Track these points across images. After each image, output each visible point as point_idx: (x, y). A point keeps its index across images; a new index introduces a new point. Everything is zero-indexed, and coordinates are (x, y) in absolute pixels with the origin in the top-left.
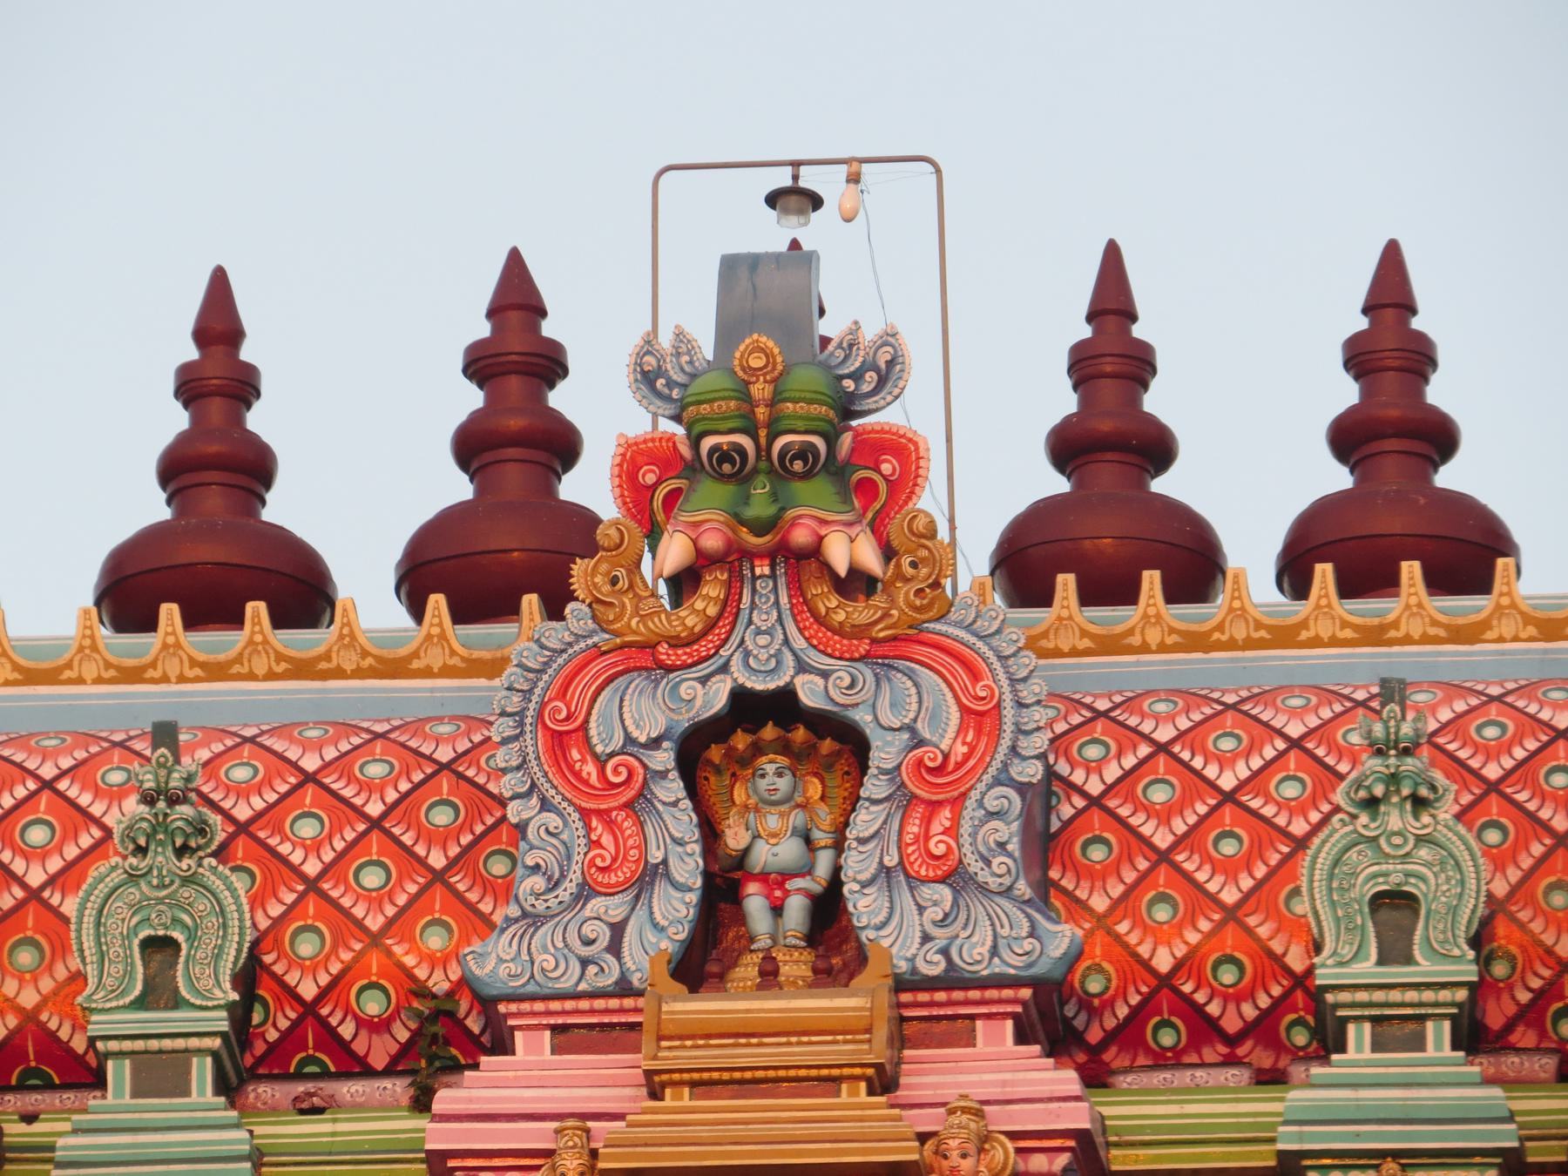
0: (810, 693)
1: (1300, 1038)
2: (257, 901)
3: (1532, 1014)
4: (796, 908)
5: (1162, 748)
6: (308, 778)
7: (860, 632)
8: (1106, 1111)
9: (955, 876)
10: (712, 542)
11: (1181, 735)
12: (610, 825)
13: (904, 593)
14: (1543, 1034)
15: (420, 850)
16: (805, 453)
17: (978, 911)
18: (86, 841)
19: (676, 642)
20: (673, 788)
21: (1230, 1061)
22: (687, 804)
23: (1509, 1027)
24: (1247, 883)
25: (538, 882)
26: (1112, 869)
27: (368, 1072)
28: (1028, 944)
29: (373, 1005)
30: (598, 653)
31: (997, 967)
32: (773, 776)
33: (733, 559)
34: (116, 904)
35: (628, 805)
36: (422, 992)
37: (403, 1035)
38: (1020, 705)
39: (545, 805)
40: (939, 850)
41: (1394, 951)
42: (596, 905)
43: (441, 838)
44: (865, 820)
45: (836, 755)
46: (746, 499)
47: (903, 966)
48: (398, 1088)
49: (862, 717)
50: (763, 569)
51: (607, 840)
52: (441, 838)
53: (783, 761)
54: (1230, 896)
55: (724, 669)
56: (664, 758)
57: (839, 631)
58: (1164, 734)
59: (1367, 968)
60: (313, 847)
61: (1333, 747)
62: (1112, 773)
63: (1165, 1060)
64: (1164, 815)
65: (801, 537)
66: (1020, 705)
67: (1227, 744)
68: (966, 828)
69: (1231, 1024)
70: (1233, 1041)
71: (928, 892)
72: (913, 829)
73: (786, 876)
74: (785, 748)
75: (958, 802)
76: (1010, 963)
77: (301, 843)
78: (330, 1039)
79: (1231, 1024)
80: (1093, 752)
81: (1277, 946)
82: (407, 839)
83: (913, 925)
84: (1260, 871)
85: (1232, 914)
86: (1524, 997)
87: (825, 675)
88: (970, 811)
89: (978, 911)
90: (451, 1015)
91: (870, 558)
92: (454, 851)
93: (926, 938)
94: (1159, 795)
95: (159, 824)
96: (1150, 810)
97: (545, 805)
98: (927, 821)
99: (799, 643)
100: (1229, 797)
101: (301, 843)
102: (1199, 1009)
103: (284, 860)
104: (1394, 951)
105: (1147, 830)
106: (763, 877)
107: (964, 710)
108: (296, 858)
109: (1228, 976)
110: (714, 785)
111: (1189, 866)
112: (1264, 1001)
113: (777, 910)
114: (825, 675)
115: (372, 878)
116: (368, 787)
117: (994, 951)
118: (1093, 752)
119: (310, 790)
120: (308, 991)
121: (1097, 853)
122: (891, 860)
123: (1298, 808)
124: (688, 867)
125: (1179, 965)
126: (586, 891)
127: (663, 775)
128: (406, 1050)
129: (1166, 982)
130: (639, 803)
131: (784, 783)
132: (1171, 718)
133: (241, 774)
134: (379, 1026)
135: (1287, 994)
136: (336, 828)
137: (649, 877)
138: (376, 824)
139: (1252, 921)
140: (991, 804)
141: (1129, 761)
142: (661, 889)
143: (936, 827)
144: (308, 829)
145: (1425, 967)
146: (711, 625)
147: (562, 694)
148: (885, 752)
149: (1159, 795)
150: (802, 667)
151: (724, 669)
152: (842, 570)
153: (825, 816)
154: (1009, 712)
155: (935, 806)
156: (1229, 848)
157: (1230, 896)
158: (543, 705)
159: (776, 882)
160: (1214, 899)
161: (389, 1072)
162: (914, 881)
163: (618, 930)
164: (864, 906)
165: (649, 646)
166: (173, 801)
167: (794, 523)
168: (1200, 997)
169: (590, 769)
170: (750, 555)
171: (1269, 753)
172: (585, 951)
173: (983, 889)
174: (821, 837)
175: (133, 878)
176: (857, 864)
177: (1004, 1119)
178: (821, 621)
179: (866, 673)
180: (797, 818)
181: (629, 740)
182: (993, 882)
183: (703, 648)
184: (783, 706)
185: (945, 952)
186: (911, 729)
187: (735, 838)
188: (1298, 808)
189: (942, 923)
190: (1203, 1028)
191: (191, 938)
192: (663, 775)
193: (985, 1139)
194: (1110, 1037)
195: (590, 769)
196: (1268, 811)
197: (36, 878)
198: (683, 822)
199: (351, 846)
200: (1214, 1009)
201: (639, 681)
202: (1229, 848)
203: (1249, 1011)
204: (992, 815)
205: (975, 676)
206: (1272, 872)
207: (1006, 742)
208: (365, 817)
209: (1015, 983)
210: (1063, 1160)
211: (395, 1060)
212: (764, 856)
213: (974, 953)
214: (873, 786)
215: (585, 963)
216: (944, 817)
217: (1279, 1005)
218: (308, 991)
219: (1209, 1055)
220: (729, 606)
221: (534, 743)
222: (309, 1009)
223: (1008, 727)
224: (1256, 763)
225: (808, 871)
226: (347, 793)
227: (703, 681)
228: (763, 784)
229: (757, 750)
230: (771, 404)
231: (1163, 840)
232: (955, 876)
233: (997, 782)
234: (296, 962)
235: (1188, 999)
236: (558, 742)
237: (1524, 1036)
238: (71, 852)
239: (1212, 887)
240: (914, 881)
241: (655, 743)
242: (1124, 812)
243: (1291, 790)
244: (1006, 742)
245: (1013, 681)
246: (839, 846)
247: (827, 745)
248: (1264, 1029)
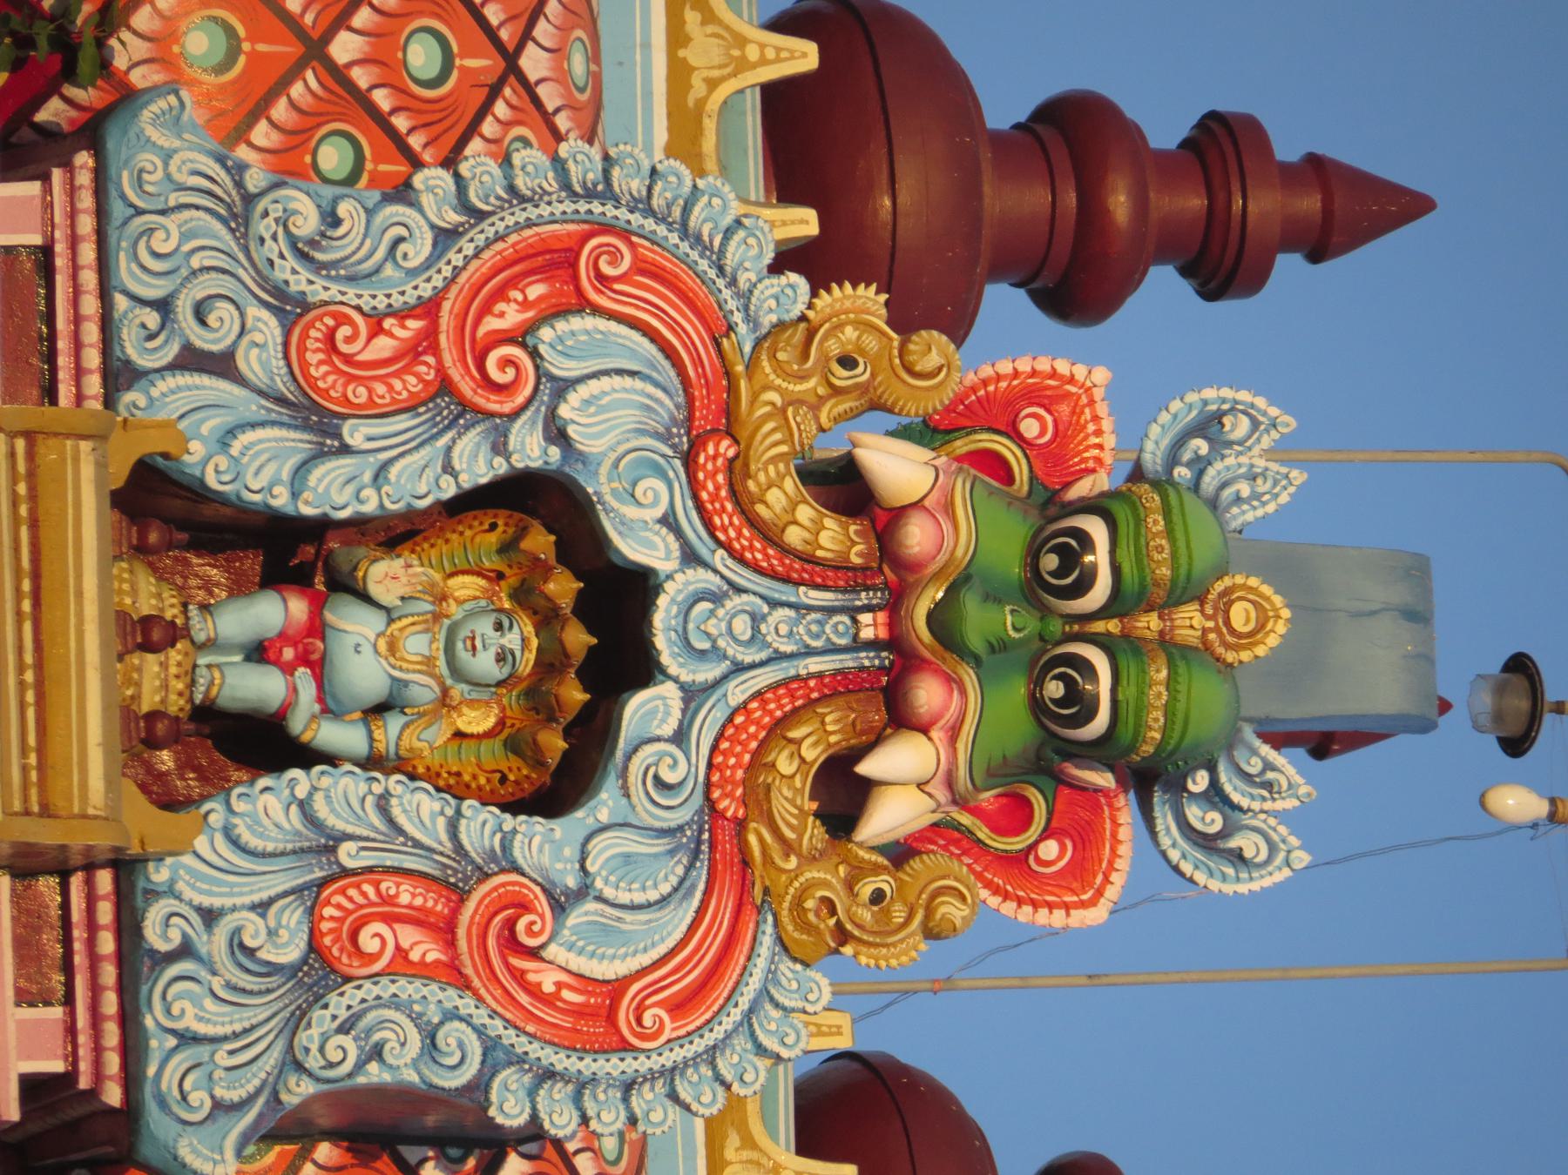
7: (757, 799)
10: (917, 536)
12: (412, 352)
13: (827, 878)
19: (737, 470)
22: (449, 490)
25: (307, 222)
28: (199, 1098)
30: (719, 330)
31: (158, 1044)
35: (445, 385)
38: (628, 1087)
39: (445, 237)
40: (368, 943)
42: (267, 327)
46: (993, 597)
47: (159, 875)
49: (605, 804)
50: (871, 627)
51: (383, 347)
53: (527, 662)
55: (691, 557)
57: (759, 762)
65: (927, 694)
66: (628, 1087)
68: (408, 988)
71: (292, 918)
72: (406, 894)
73: (319, 667)
74: (550, 664)
75: (452, 973)
88: (436, 997)
90: (69, 73)
92: (361, 77)
93: (210, 917)
97: (445, 237)
98: (418, 919)
99: (737, 692)
106: (317, 628)
113: (259, 652)
114: (680, 737)
117: (187, 1039)
122: (349, 856)
127: (500, 448)
131: (484, 664)
140: (451, 1034)
142: (297, 442)
143: (408, 935)
146: (769, 534)
147: (644, 268)
150: (693, 695)
151: (691, 557)
152: (866, 768)
153: (427, 740)
154: (614, 1066)
155: (445, 931)
158: (625, 234)
162: (313, 894)
163: (222, 365)
165: (729, 423)
167: (952, 681)
169: (509, 316)
170: (895, 604)
172: (184, 308)
173: (298, 1020)
178: (778, 729)
180: (423, 690)
181: (563, 387)
182: (309, 1037)
183: (728, 519)
185: (185, 950)
186: (583, 892)
189: (241, 949)
192: (500, 448)
195: (509, 316)
201: (668, 405)
209: (131, 1078)
215: (164, 306)
216: (427, 950)
223: (587, 1065)
225: (329, 708)
227: (669, 521)
228: (484, 626)
229: (547, 618)
230: (1167, 643)
233: (490, 1045)
240: (313, 894)
241: (557, 434)
245: (670, 1073)
246: (373, 762)
247: (554, 743)
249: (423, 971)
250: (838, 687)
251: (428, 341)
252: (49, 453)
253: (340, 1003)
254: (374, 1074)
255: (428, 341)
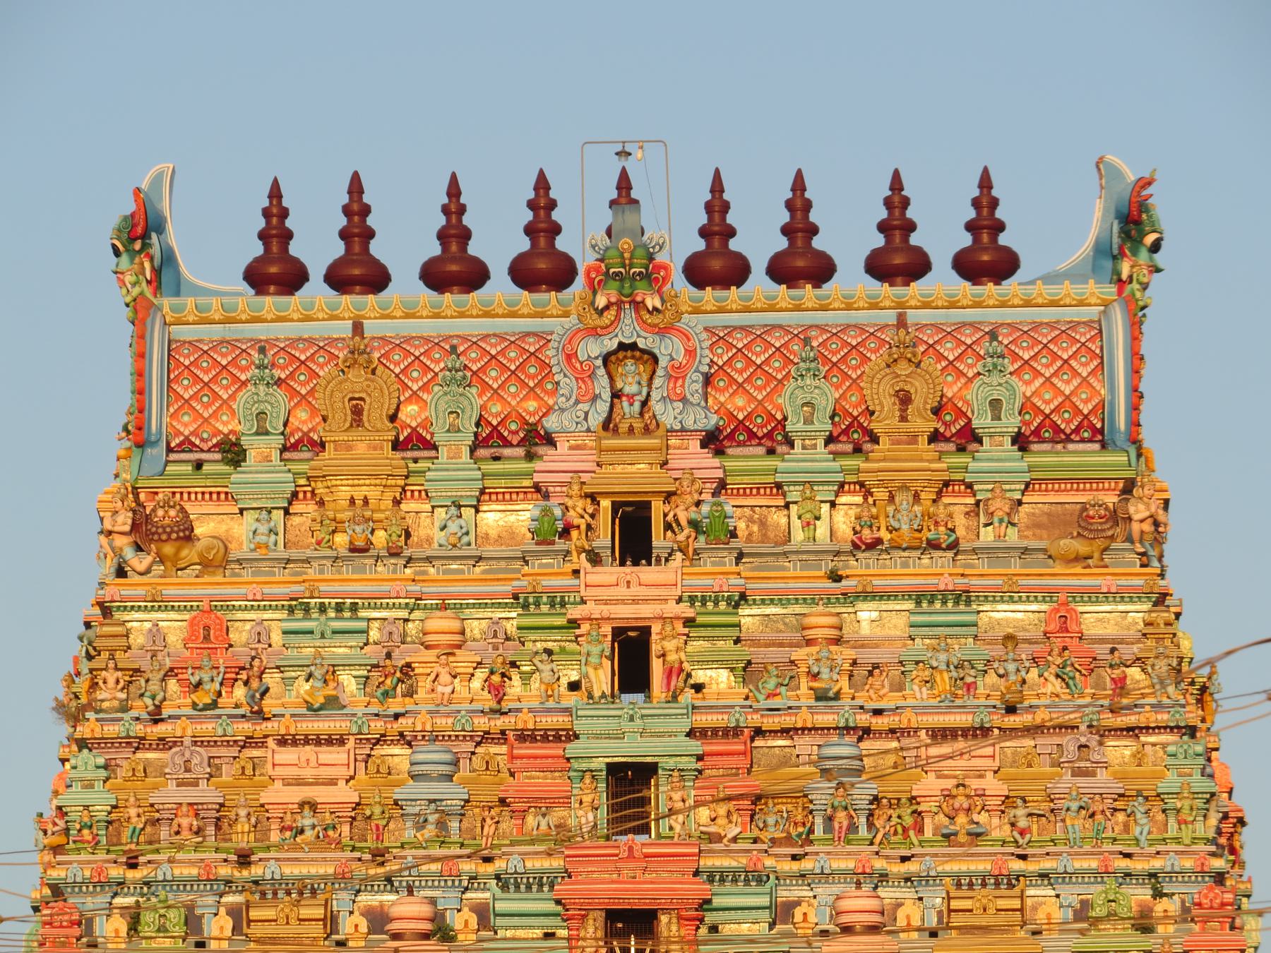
0: (641, 344)
1: (779, 438)
2: (480, 396)
3: (845, 432)
4: (637, 405)
5: (739, 350)
6: (493, 357)
7: (655, 326)
8: (726, 464)
9: (683, 399)
10: (613, 300)
11: (745, 346)
12: (584, 382)
13: (668, 314)
14: (849, 438)
15: (526, 381)
16: (641, 273)
17: (690, 410)
18: (429, 377)
19: (602, 328)
20: (601, 371)
21: (759, 444)
22: (606, 376)
23: (839, 435)
24: (764, 393)
25: (563, 399)
26: (726, 389)
27: (512, 445)
28: (705, 420)
29: (513, 427)
30: (579, 330)
31: (696, 427)
32: (630, 366)
33: (619, 304)
34: (441, 401)
35: (589, 376)
36: (527, 423)
37: (522, 435)
38: (702, 348)
39: (565, 376)
40: (679, 392)
41: (808, 421)
42: (580, 406)
43: (532, 377)
44: (657, 382)
45: (648, 360)
47: (669, 427)
48: (520, 451)
49: (656, 351)
50: (627, 306)
51: (583, 386)
52: (532, 377)
53: (633, 361)
54: (760, 397)
55: (616, 336)
56: (599, 362)
57: (649, 325)
58: (740, 345)
59: (800, 426)
60: (496, 379)
61: (789, 350)
62: (725, 358)
63: (740, 444)
64: (741, 372)
65: (639, 299)
66: (702, 348)
67: (758, 349)
68: (686, 385)
69: (760, 434)
70: (760, 439)
71: (676, 404)
72: (671, 385)
73: (634, 395)
74: (633, 357)
75: (684, 378)
76: (700, 426)
77: (492, 378)
78: (501, 436)
79: (760, 434)
80: (720, 351)
81: (773, 412)
82: (523, 377)
83: (672, 414)
84: (768, 390)
85: (760, 402)
86: (844, 427)
87: (646, 338)
88: (688, 380)
89: (690, 410)
90: (536, 430)
91: (658, 304)
92: (536, 381)
93: (675, 418)
94: (739, 365)
95: (453, 378)
96: (736, 370)
97: (565, 376)
98: (675, 383)
99: (638, 328)
100: (759, 366)
101: (492, 378)
102: (751, 430)
103: (487, 384)
104: (808, 421)
105: (736, 377)
106: (627, 396)
107: (686, 350)
108: (490, 383)
109: (759, 420)
110: (612, 367)
111: (748, 388)
112: (769, 428)
113: (631, 404)
114: (646, 338)
115: (513, 389)
116: (510, 360)
117: (695, 422)
118: (720, 351)
119: (494, 361)
120: (495, 423)
121: (722, 384)
122: (665, 395)
123: (779, 370)
124: (607, 395)
125: (745, 418)
126: (577, 402)
128: (522, 440)
129: (741, 422)
130: (592, 376)
131: (633, 368)
132: (742, 340)
133: (473, 355)
134: (516, 433)
135: (776, 426)
136: (502, 374)
137: (595, 398)
138: (513, 372)
139: (766, 405)
140: (694, 379)
141: (730, 354)
142: (599, 401)
143: (678, 385)
144: (493, 373)
145: (817, 426)
148: (663, 362)
149: (739, 365)
150: (639, 336)
151: (616, 336)
153: (645, 377)
154: (698, 351)
155: (677, 379)
156: (759, 382)
157: (760, 397)
159: (631, 398)
160: (755, 398)
161: (518, 445)
163: (586, 414)
164: (657, 407)
165: (594, 329)
166: (457, 371)
167: (637, 294)
168: (751, 427)
169: (578, 365)
170: (624, 302)
171: (770, 352)
172: (578, 420)
173: (691, 403)
174: (644, 383)
175: (446, 394)
176: (655, 395)
177: (698, 474)
179: (657, 338)
180: (637, 378)
181: (589, 356)
182: (694, 402)
183: (610, 329)
184: (634, 346)
185: (681, 422)
186: (670, 355)
187: (619, 385)
188: (779, 370)
189: (680, 413)
190: (752, 435)
191: (463, 412)
193: (693, 481)
194: (725, 437)
195: (578, 365)
196: (770, 371)
197: (415, 388)
198: (605, 381)
199: (506, 379)
200: (755, 430)
201: (592, 339)
202: (759, 382)
203: (765, 431)
204: (693, 382)
205: (689, 340)
206: (772, 390)
207: (698, 360)
208: (510, 370)
209: (701, 431)
210: (715, 485)
211: (519, 442)
212: (627, 390)
213: (689, 423)
214: (660, 372)
215: (577, 423)
216: (680, 382)
217: (773, 429)
218: (495, 423)
219: (753, 443)
220: (618, 317)
221: (561, 357)
222: (495, 428)
223: (698, 355)
224: (767, 355)
225: (640, 393)
226: (505, 362)
227: (610, 339)
229: (625, 357)
230: (631, 259)
231: (740, 380)
232: (683, 399)
233: (695, 371)
234: (491, 414)
235: (747, 427)
236: (569, 357)
237: (843, 438)
238: (425, 380)
239: (755, 394)
241: (596, 358)
242: (729, 371)
243: (777, 364)
244: (698, 360)
245: (700, 341)
247: (646, 357)
248: (769, 435)
249: (684, 382)
250: (637, 311)
251: (582, 379)
252: (603, 448)
253: (689, 396)
254: (700, 391)
255: (582, 379)
